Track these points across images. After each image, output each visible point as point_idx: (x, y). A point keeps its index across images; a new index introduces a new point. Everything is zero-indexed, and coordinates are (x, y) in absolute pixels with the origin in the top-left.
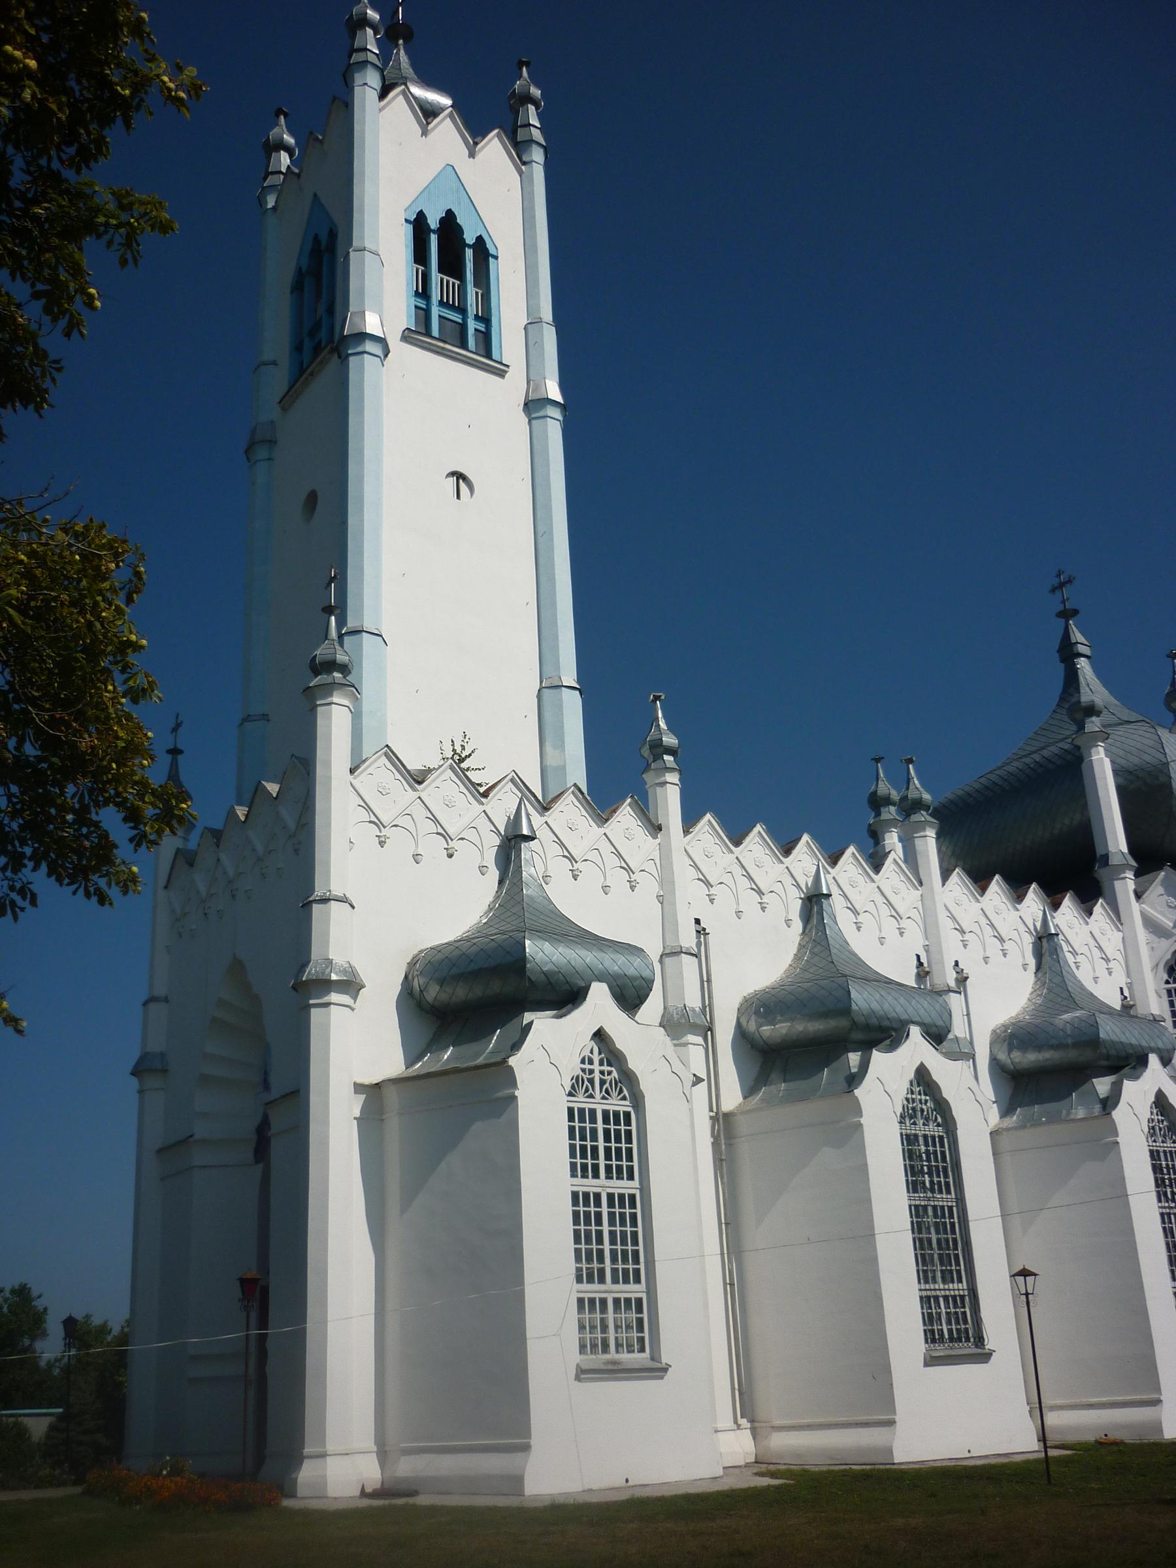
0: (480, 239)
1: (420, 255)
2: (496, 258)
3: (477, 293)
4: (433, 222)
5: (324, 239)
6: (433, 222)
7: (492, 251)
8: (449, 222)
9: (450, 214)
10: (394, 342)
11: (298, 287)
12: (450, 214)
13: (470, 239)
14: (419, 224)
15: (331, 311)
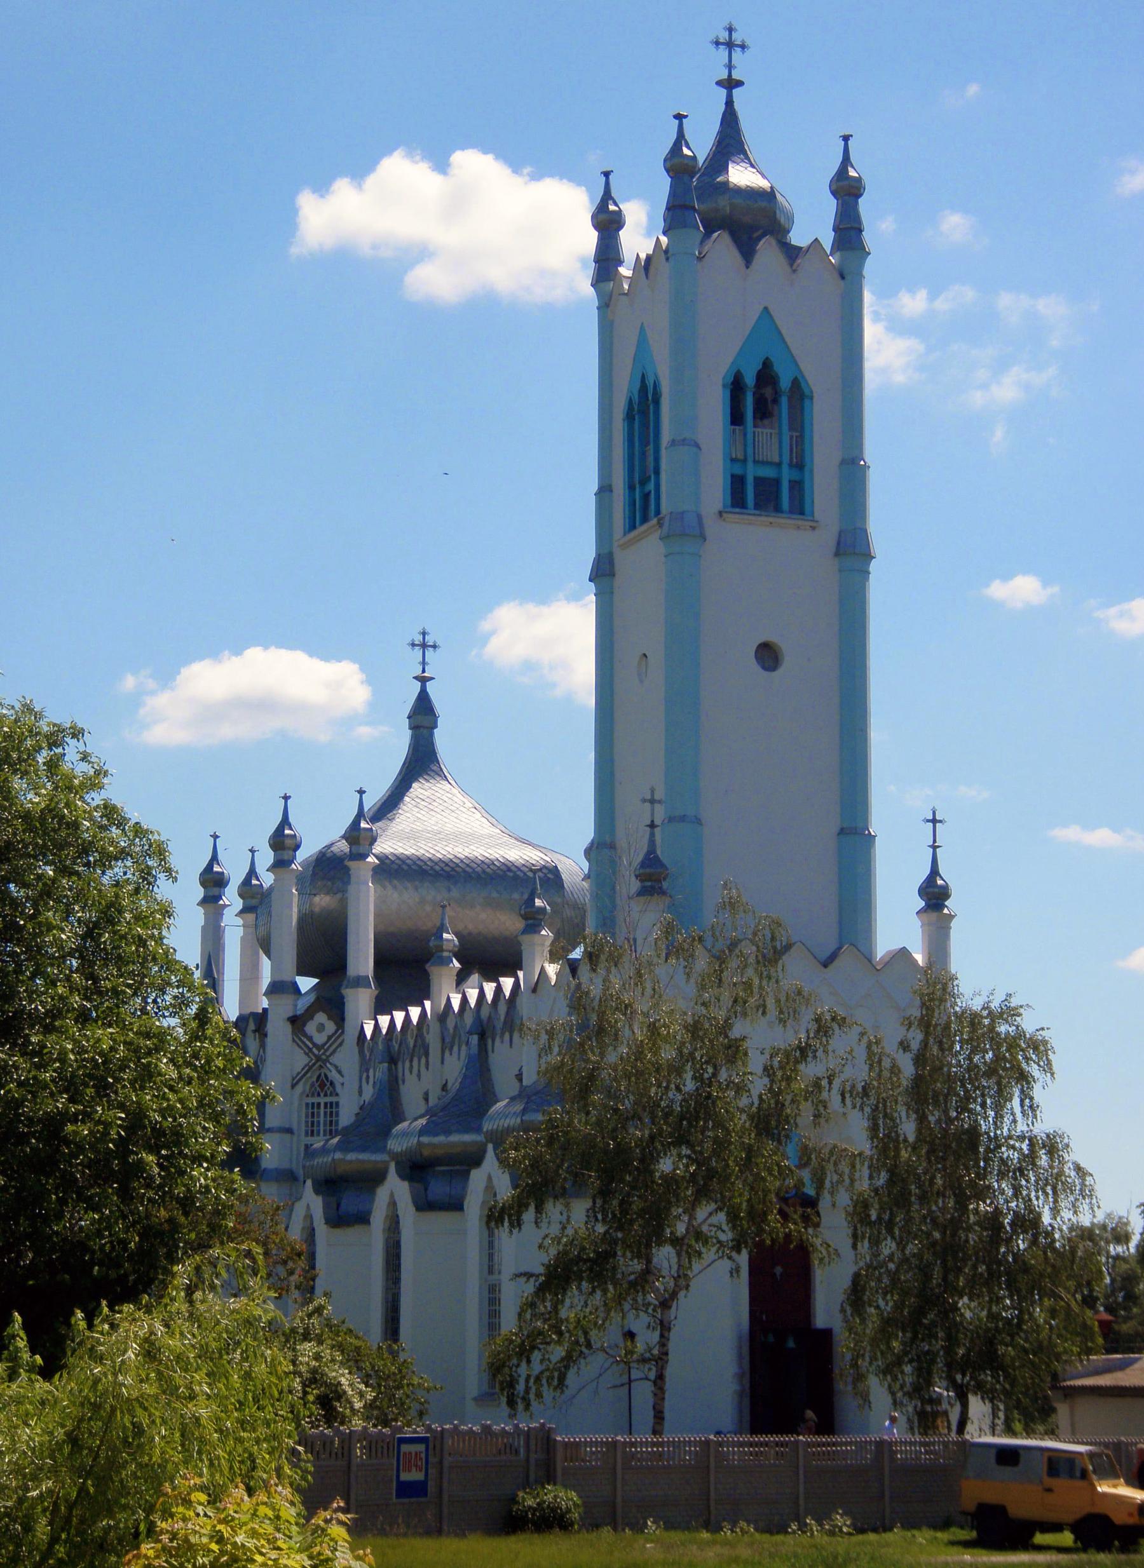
0: (796, 384)
1: (736, 418)
2: (812, 398)
3: (791, 437)
4: (750, 380)
5: (650, 383)
6: (750, 380)
7: (807, 392)
8: (766, 376)
9: (767, 364)
10: (712, 527)
11: (629, 417)
12: (767, 364)
13: (785, 383)
14: (736, 387)
15: (657, 472)
